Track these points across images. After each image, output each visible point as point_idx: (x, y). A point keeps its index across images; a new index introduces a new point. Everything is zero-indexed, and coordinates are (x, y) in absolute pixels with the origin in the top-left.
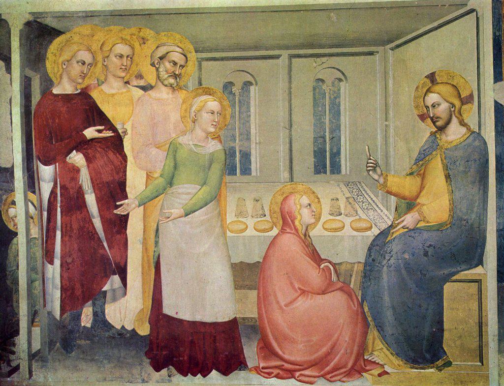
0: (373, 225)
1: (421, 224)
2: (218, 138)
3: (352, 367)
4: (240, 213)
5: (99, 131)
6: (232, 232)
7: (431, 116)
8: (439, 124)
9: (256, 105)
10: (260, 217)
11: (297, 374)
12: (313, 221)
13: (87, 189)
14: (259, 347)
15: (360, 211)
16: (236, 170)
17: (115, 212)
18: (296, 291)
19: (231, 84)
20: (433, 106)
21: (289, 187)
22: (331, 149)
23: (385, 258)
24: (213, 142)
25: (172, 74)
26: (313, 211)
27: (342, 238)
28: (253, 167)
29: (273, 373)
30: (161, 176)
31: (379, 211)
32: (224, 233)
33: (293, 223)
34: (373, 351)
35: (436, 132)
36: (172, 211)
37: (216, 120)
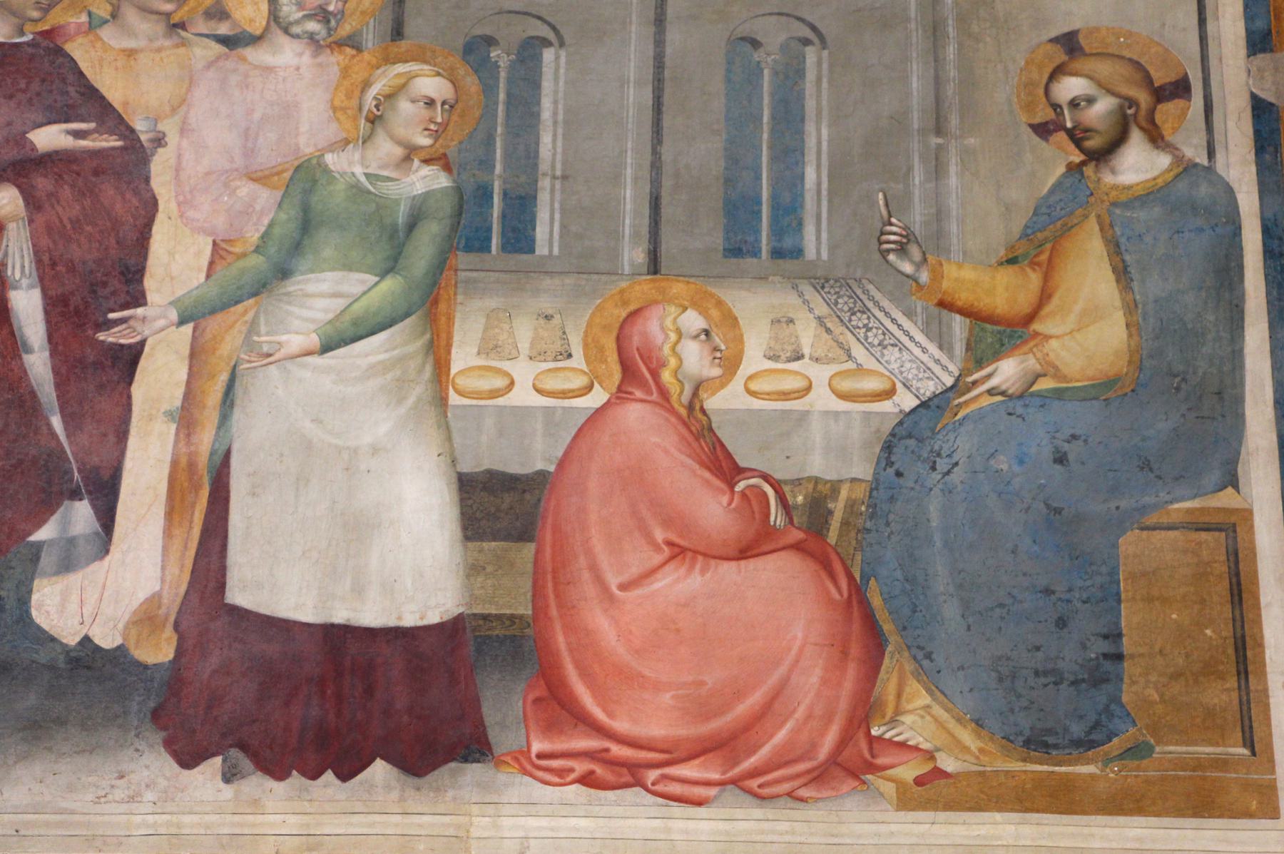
0: (899, 386)
1: (1044, 384)
2: (442, 161)
3: (834, 761)
4: (489, 347)
5: (78, 134)
6: (460, 393)
7: (1069, 125)
8: (1093, 143)
9: (556, 92)
10: (555, 360)
11: (652, 775)
12: (716, 372)
13: (18, 276)
14: (531, 697)
15: (859, 352)
16: (489, 239)
17: (101, 336)
18: (657, 548)
19: (490, 41)
20: (1074, 104)
21: (644, 288)
22: (774, 197)
23: (934, 468)
24: (426, 170)
25: (317, 11)
26: (716, 349)
27: (804, 416)
28: (541, 233)
29: (572, 770)
30: (257, 250)
31: (917, 351)
32: (442, 401)
33: (655, 374)
34: (898, 712)
35: (1083, 163)
36: (284, 338)
37: (439, 120)
